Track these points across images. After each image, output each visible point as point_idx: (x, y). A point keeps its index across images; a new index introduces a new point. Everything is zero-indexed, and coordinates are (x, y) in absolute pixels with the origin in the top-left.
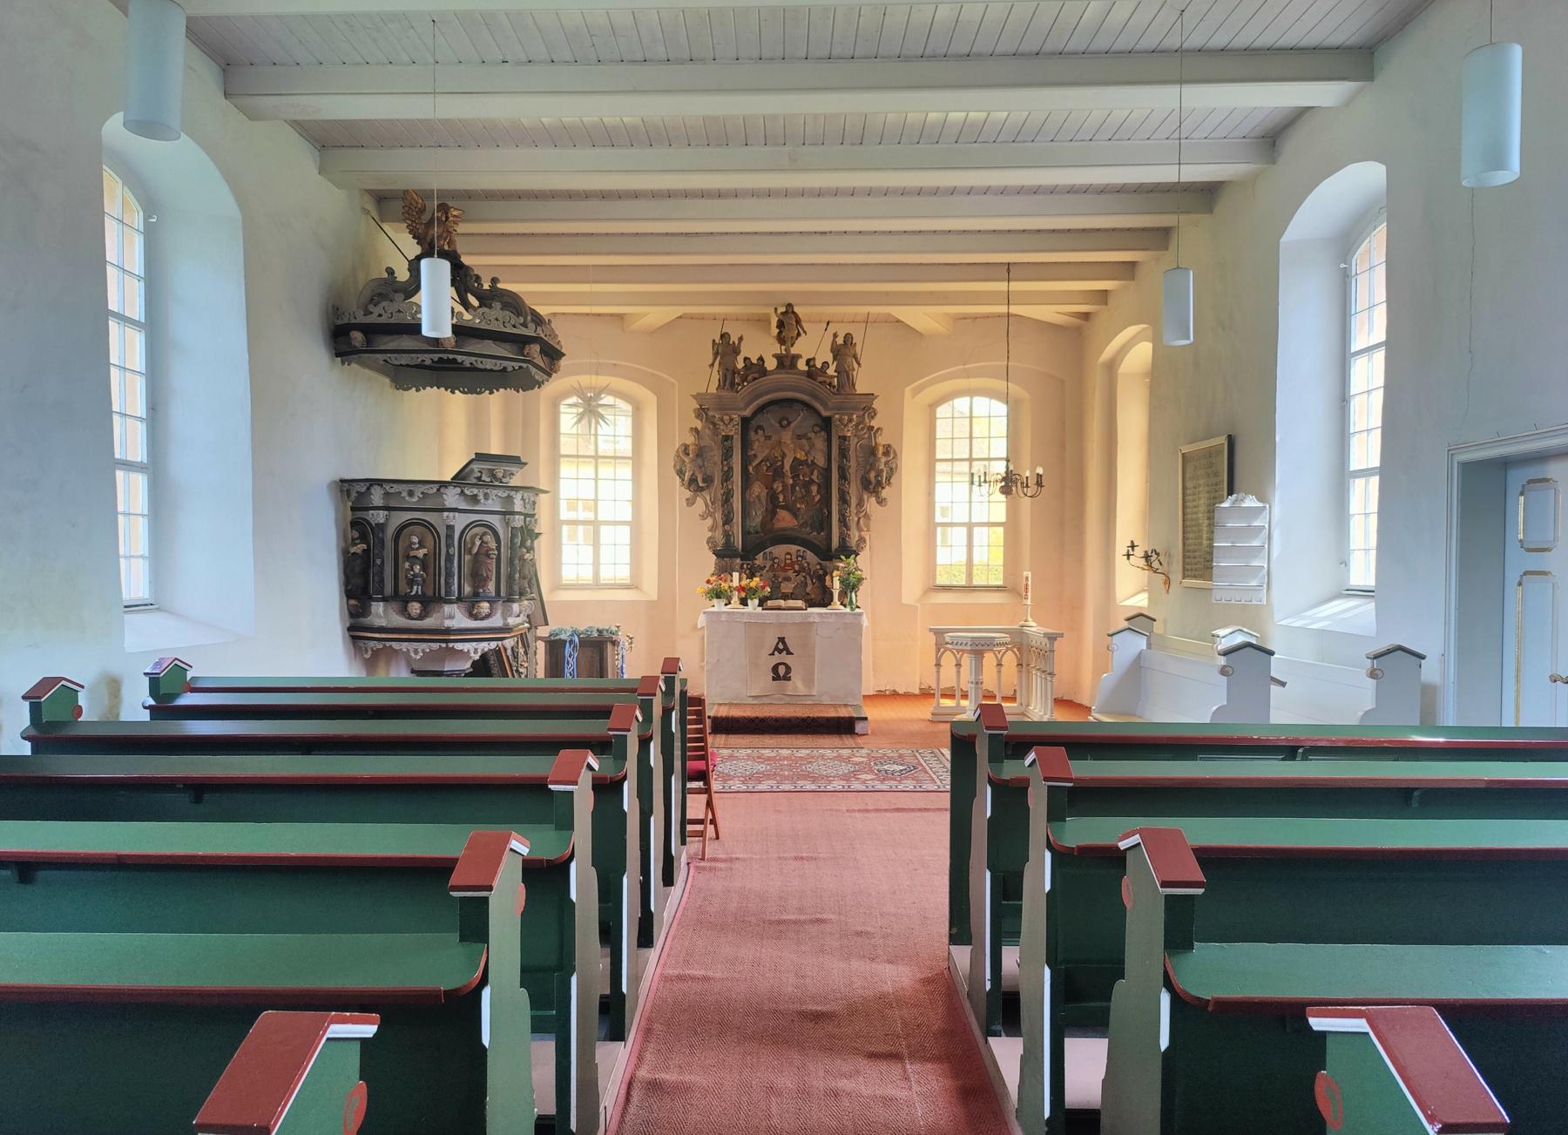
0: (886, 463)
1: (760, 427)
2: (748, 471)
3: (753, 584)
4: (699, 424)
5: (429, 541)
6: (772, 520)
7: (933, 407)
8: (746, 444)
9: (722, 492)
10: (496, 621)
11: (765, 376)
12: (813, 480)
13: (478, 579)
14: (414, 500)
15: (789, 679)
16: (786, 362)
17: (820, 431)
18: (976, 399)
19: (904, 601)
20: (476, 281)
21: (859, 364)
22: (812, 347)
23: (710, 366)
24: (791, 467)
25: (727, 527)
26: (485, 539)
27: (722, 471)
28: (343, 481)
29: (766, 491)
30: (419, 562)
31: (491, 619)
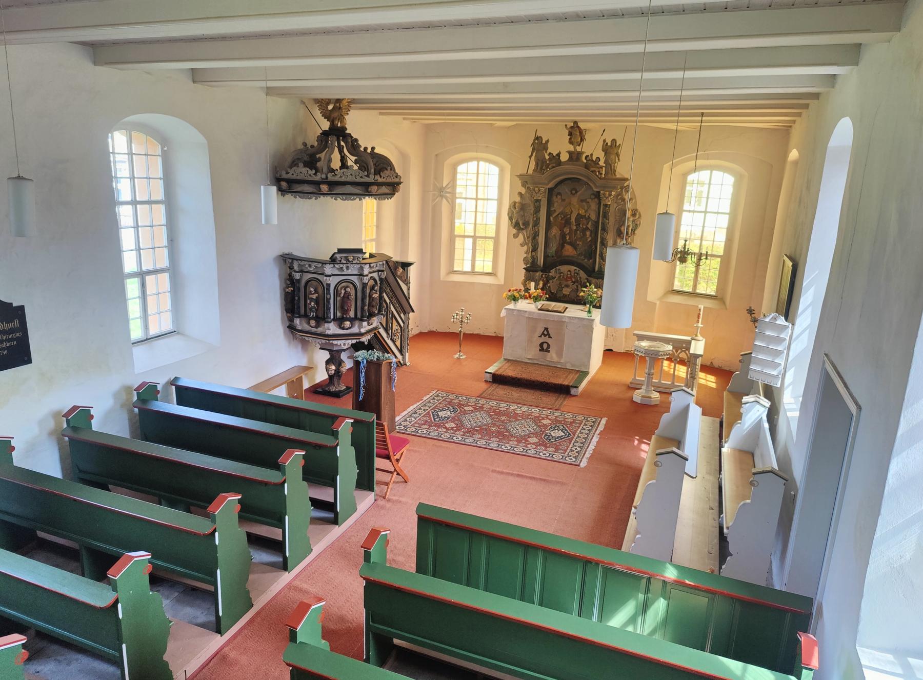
0: (634, 221)
1: (559, 194)
2: (549, 219)
4: (523, 191)
5: (320, 290)
7: (685, 175)
8: (550, 204)
10: (355, 330)
11: (560, 165)
12: (588, 228)
13: (345, 311)
14: (311, 269)
15: (549, 352)
16: (575, 157)
17: (595, 198)
18: (715, 172)
19: (649, 299)
20: (355, 142)
21: (619, 159)
22: (592, 148)
25: (534, 253)
26: (348, 290)
27: (533, 220)
28: (281, 256)
29: (560, 232)
30: (314, 301)
31: (352, 329)
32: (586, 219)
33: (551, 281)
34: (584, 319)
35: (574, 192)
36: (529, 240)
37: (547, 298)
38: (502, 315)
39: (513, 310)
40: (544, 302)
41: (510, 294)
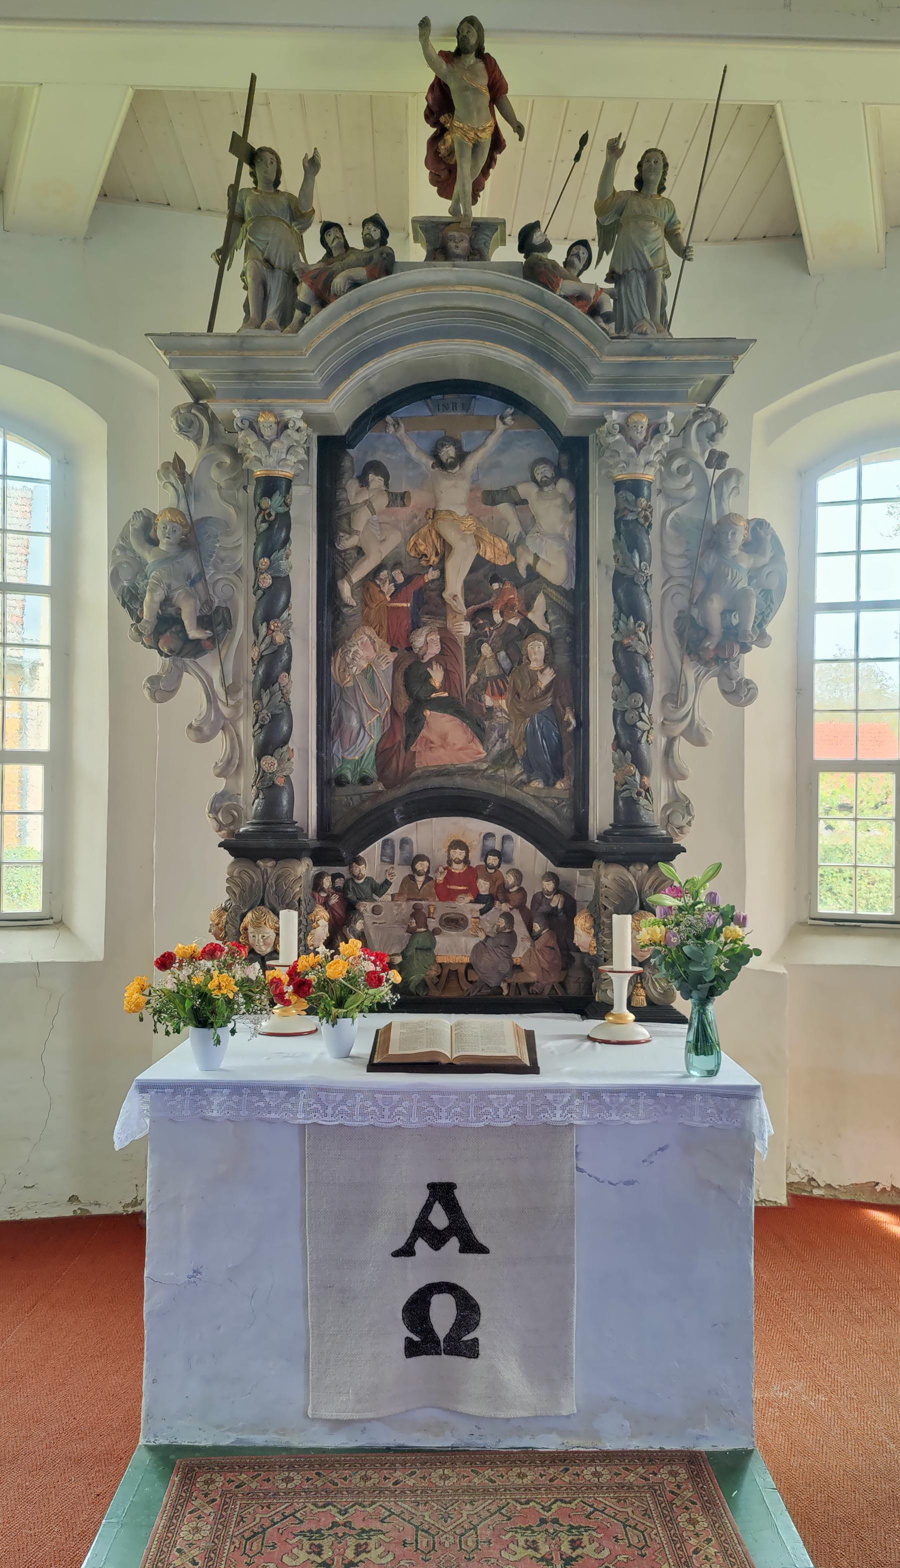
0: (754, 574)
1: (376, 467)
3: (336, 970)
4: (191, 456)
6: (407, 748)
9: (255, 653)
11: (388, 272)
15: (472, 1350)
17: (554, 480)
23: (219, 252)
24: (468, 587)
25: (270, 763)
27: (257, 588)
29: (392, 657)
32: (518, 587)
33: (365, 907)
34: (689, 1093)
35: (449, 452)
36: (236, 707)
37: (395, 989)
38: (120, 1138)
39: (198, 1089)
40: (381, 1020)
41: (166, 981)
